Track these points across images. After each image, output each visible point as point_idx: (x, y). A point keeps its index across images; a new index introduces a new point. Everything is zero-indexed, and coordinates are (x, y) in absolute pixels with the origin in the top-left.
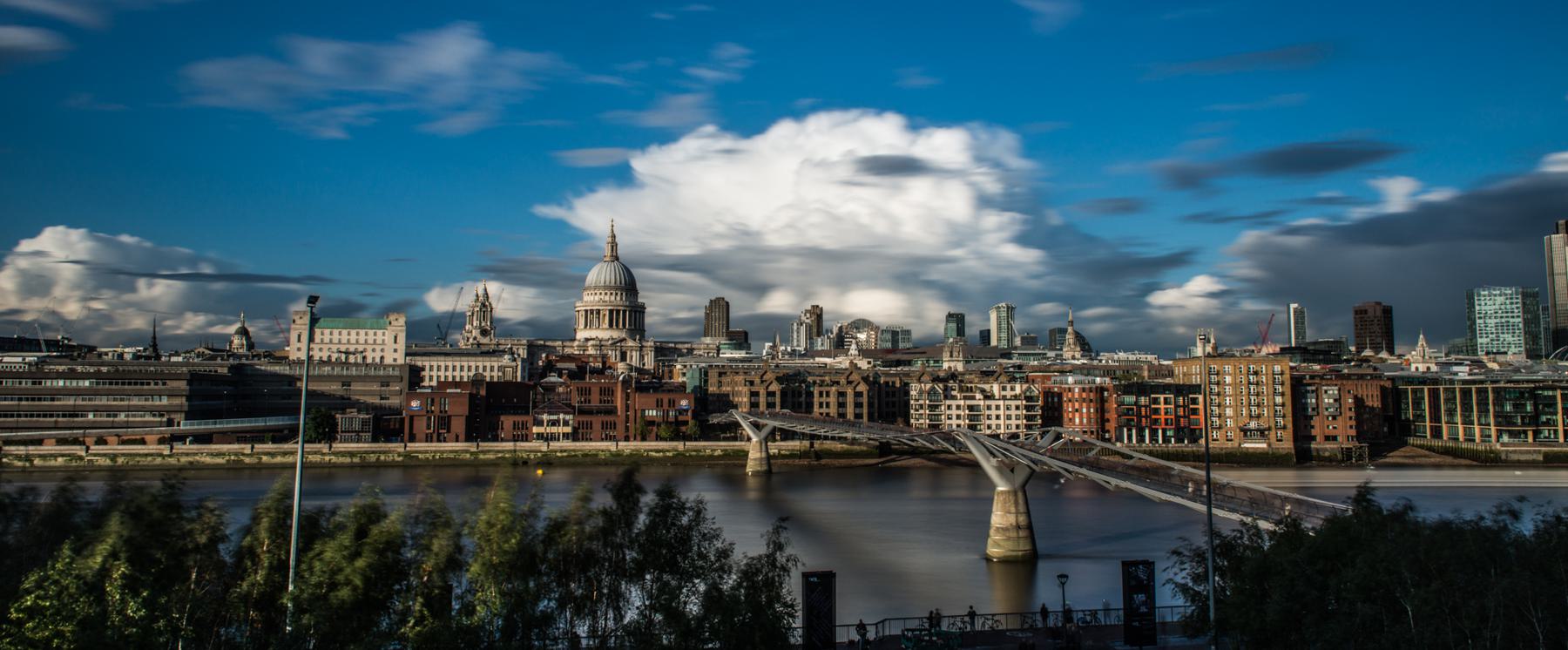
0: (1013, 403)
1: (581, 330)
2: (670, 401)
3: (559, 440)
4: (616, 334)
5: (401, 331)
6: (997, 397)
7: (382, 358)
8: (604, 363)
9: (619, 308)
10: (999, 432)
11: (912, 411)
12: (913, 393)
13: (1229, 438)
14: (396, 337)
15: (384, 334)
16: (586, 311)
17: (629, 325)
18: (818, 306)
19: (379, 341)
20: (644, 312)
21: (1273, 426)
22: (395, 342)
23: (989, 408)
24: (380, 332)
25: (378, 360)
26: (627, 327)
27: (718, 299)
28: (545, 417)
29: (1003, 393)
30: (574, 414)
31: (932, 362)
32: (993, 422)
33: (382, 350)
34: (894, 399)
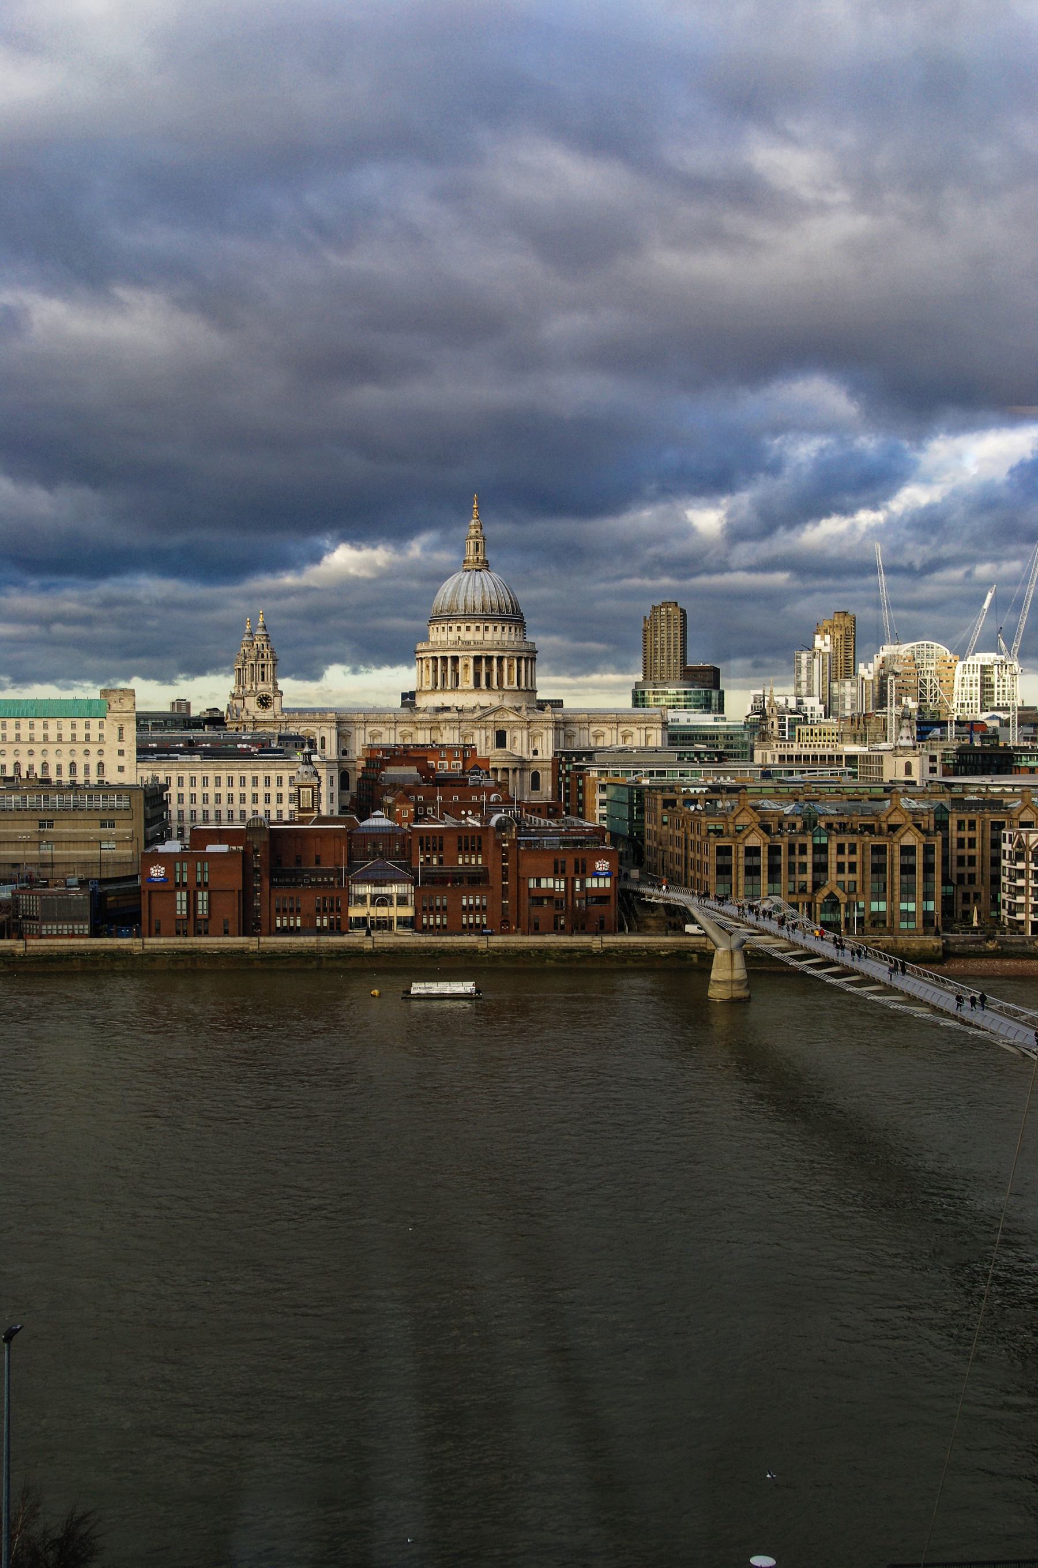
1: (427, 692)
3: (390, 928)
4: (485, 699)
5: (128, 720)
8: (465, 760)
9: (490, 654)
12: (1006, 846)
14: (121, 729)
16: (435, 659)
17: (510, 683)
18: (845, 613)
20: (534, 659)
22: (121, 738)
24: (94, 723)
26: (505, 686)
27: (666, 605)
28: (367, 890)
30: (415, 883)
33: (101, 752)
34: (972, 852)
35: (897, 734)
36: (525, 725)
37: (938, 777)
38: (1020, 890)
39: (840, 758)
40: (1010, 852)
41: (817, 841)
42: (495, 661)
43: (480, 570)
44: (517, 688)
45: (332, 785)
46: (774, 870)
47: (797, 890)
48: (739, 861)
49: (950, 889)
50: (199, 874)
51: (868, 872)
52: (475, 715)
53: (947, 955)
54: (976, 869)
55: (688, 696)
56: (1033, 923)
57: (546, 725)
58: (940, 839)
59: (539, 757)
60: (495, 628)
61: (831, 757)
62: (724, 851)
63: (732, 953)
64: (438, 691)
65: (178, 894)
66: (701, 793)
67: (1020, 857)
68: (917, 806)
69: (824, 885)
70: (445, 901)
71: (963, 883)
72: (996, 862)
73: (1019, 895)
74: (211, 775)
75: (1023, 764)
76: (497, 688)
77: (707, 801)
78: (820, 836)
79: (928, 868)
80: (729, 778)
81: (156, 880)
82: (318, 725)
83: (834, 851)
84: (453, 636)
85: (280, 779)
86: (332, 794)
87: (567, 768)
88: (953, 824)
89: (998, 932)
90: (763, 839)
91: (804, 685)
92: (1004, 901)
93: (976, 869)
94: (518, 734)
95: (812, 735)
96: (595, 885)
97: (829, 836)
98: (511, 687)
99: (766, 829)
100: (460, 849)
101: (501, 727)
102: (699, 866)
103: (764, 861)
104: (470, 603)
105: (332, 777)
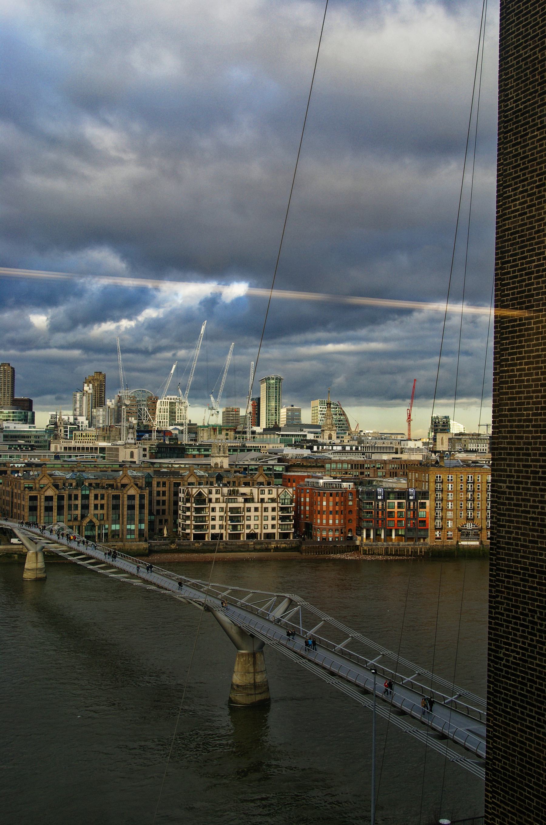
0: (270, 506)
6: (256, 500)
10: (257, 531)
11: (180, 512)
12: (181, 495)
13: (449, 536)
18: (100, 373)
21: (484, 527)
23: (249, 510)
29: (261, 496)
31: (203, 450)
32: (252, 523)
35: (126, 436)
37: (147, 459)
38: (188, 518)
39: (96, 448)
40: (183, 498)
41: (84, 492)
46: (60, 508)
47: (73, 519)
48: (41, 504)
49: (153, 517)
51: (111, 509)
53: (151, 552)
54: (166, 507)
55: (15, 415)
56: (194, 534)
58: (148, 491)
61: (92, 448)
62: (33, 499)
63: (37, 554)
66: (21, 467)
67: (188, 501)
68: (136, 474)
69: (87, 516)
71: (159, 514)
72: (176, 503)
73: (187, 520)
75: (190, 453)
77: (24, 471)
78: (85, 490)
79: (142, 507)
80: (36, 459)
83: (93, 498)
88: (155, 484)
89: (176, 539)
90: (55, 492)
91: (78, 410)
92: (180, 523)
93: (166, 507)
95: (82, 436)
97: (90, 490)
99: (56, 486)
102: (19, 506)
103: (55, 503)
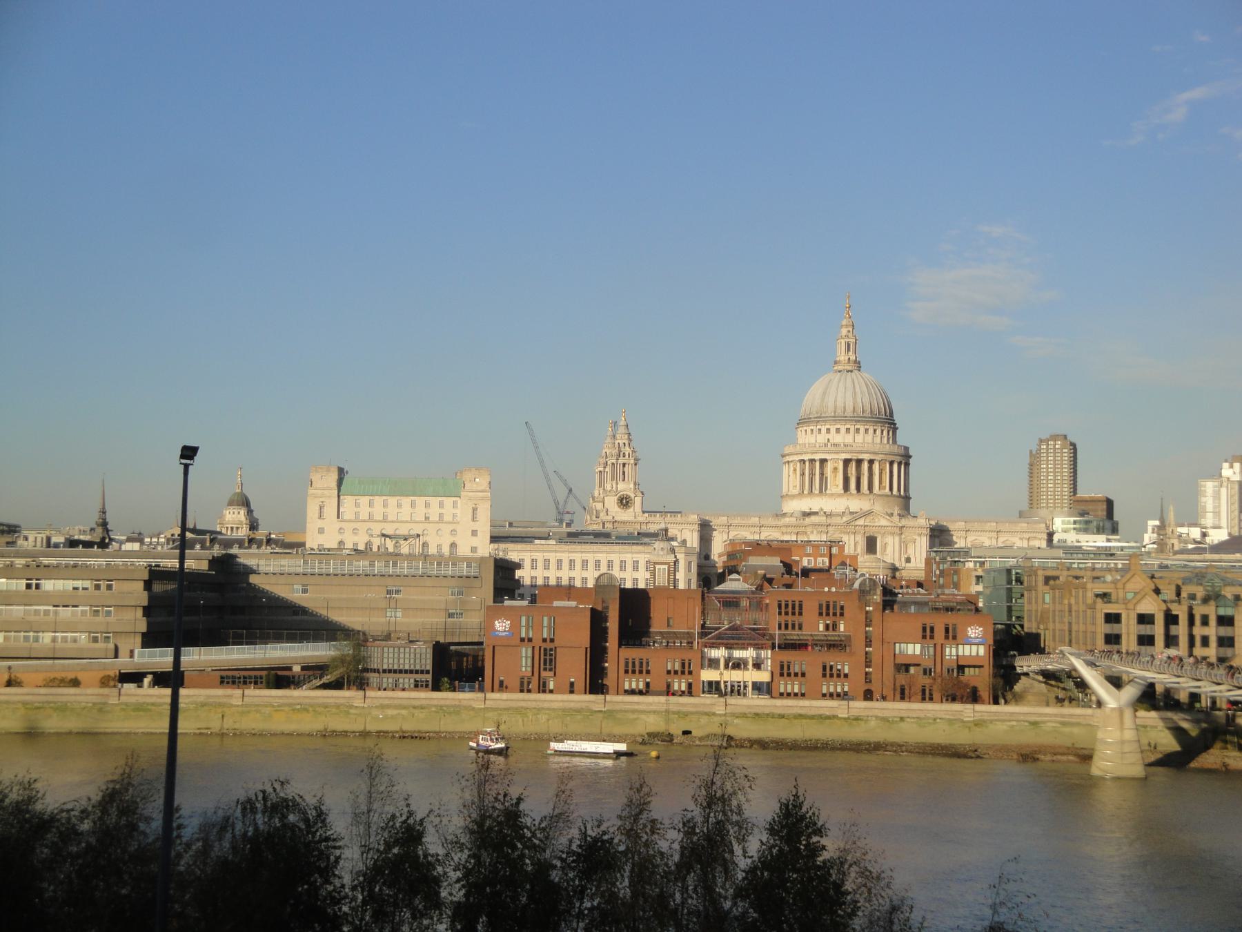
1: (793, 497)
2: (947, 630)
4: (856, 504)
5: (483, 499)
7: (453, 545)
14: (475, 510)
15: (455, 505)
16: (804, 461)
19: (448, 518)
22: (474, 519)
24: (448, 502)
25: (446, 551)
27: (1054, 438)
28: (719, 653)
30: (773, 647)
33: (453, 532)
36: (897, 530)
41: (1222, 612)
42: (865, 466)
43: (851, 371)
44: (890, 493)
45: (690, 570)
48: (1129, 630)
50: (545, 630)
52: (845, 519)
57: (918, 531)
59: (912, 564)
60: (867, 430)
64: (806, 496)
65: (524, 650)
70: (804, 666)
74: (565, 557)
76: (868, 492)
81: (500, 634)
82: (680, 527)
84: (822, 438)
85: (635, 564)
86: (690, 581)
87: (941, 568)
94: (889, 539)
96: (967, 653)
98: (882, 492)
100: (821, 614)
101: (870, 532)
103: (1158, 630)
104: (840, 404)
105: (690, 563)
